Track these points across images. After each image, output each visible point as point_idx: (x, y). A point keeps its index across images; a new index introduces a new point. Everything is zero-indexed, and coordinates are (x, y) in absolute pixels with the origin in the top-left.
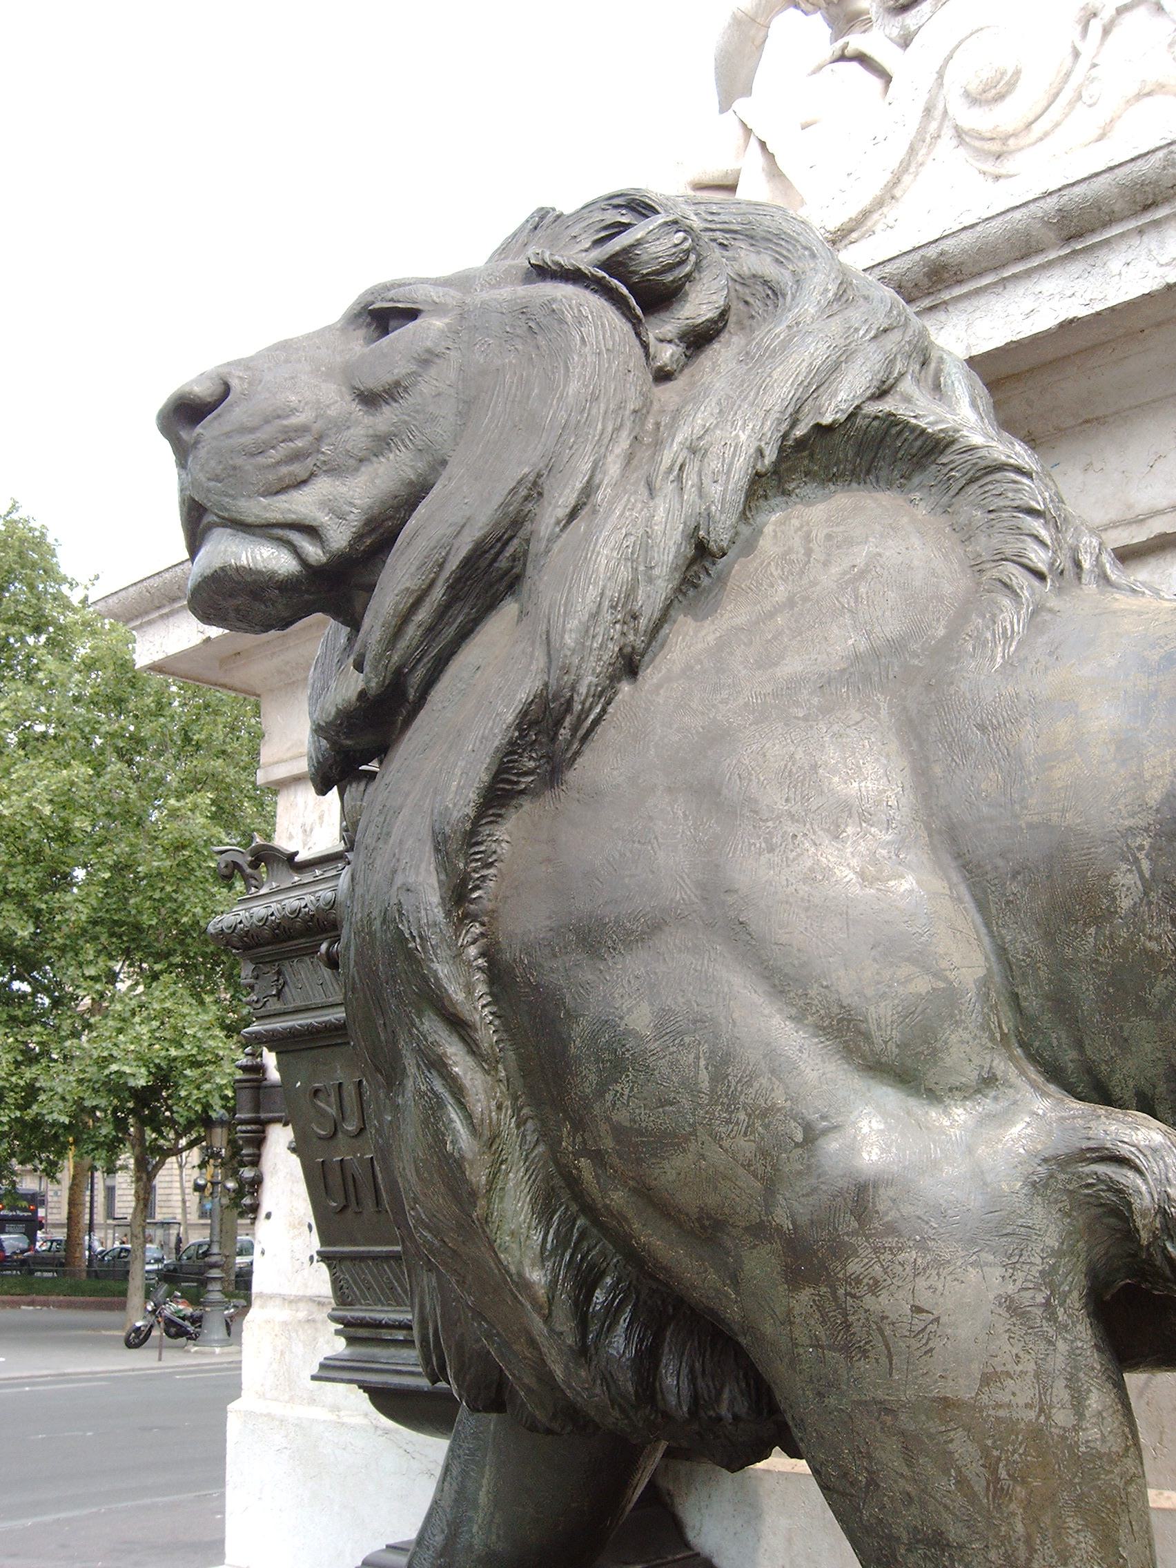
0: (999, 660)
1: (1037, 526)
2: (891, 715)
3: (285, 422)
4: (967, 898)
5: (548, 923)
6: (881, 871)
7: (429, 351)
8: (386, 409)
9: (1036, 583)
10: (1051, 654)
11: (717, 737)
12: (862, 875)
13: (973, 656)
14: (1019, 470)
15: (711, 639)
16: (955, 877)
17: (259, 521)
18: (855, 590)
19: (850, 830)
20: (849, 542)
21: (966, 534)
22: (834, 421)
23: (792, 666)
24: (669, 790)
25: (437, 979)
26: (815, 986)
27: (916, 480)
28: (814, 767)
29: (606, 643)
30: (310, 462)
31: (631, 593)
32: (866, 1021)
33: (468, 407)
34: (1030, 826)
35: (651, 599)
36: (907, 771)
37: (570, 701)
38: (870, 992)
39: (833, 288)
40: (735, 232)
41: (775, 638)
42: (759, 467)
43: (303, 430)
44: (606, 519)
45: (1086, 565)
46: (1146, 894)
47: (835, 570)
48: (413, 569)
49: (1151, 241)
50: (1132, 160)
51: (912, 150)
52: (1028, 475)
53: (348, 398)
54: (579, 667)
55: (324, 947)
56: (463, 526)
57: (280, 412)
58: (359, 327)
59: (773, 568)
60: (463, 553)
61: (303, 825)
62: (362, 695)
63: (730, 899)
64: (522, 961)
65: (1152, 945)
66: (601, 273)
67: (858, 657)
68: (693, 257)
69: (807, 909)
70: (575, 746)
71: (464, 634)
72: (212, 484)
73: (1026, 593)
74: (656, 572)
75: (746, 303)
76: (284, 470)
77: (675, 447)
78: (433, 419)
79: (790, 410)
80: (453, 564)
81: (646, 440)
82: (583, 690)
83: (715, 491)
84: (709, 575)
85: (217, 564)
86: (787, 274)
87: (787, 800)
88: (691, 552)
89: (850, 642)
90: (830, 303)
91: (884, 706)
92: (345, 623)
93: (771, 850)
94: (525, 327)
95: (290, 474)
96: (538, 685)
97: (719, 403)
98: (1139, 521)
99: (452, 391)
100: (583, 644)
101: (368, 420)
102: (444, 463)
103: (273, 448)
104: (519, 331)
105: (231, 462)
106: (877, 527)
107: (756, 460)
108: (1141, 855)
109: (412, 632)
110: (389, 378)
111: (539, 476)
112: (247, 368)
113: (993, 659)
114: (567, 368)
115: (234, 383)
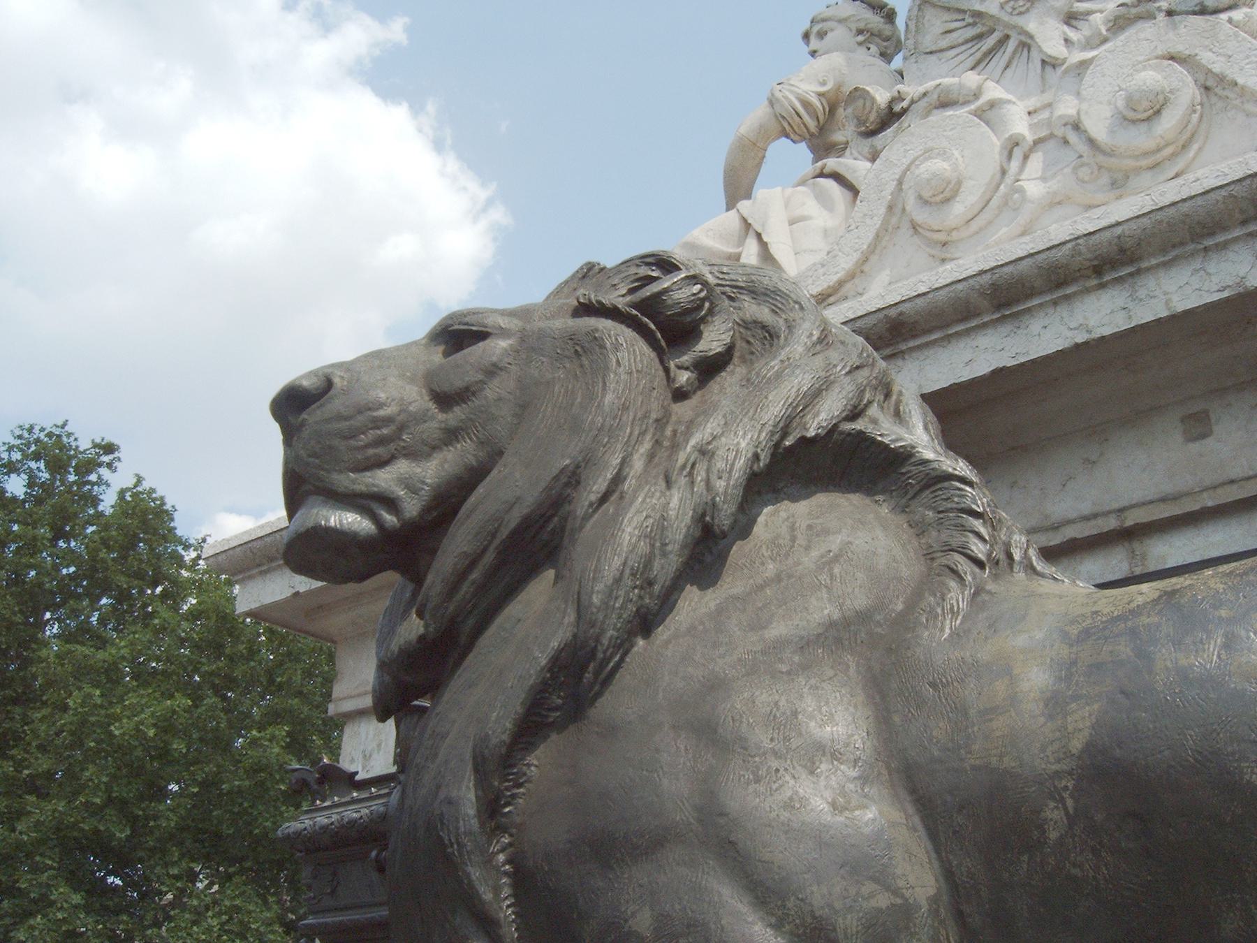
0: (947, 631)
1: (978, 525)
2: (858, 672)
3: (375, 414)
4: (920, 827)
6: (849, 802)
7: (494, 365)
9: (977, 570)
10: (990, 626)
11: (716, 686)
12: (834, 805)
13: (926, 627)
14: (963, 480)
15: (712, 605)
16: (911, 809)
18: (831, 570)
19: (824, 767)
20: (826, 532)
21: (920, 529)
22: (817, 435)
23: (778, 630)
24: (674, 727)
25: (470, 881)
26: (792, 899)
27: (880, 486)
28: (795, 714)
29: (626, 602)
30: (392, 447)
31: (648, 562)
32: (835, 930)
33: (523, 408)
34: (974, 768)
35: (664, 569)
36: (871, 720)
37: (593, 652)
38: (838, 905)
39: (816, 334)
40: (741, 288)
41: (765, 606)
42: (755, 467)
43: (388, 420)
44: (631, 504)
45: (1017, 556)
46: (1071, 828)
47: (815, 553)
49: (1063, 310)
50: (1048, 249)
51: (878, 237)
52: (971, 484)
53: (427, 398)
54: (603, 622)
55: (374, 854)
58: (439, 344)
59: (764, 550)
60: (513, 525)
61: (364, 751)
62: (422, 638)
63: (722, 821)
65: (1074, 871)
66: (635, 312)
67: (831, 625)
68: (707, 305)
69: (786, 832)
70: (597, 688)
71: (511, 592)
72: (311, 460)
73: (969, 578)
74: (669, 548)
75: (748, 342)
76: (371, 451)
77: (689, 449)
79: (781, 425)
80: (504, 533)
81: (665, 441)
82: (605, 642)
83: (720, 485)
84: (711, 553)
85: (310, 523)
86: (781, 322)
87: (772, 740)
88: (698, 533)
89: (826, 612)
90: (814, 345)
91: (853, 666)
92: (411, 580)
93: (757, 781)
95: (375, 455)
96: (569, 635)
97: (724, 416)
98: (1055, 528)
99: (511, 397)
100: (606, 604)
101: (441, 416)
102: (501, 453)
104: (567, 353)
106: (850, 522)
107: (753, 463)
108: (1066, 795)
109: (466, 588)
111: (578, 467)
112: (348, 370)
113: (942, 630)
114: (604, 383)
115: (336, 380)
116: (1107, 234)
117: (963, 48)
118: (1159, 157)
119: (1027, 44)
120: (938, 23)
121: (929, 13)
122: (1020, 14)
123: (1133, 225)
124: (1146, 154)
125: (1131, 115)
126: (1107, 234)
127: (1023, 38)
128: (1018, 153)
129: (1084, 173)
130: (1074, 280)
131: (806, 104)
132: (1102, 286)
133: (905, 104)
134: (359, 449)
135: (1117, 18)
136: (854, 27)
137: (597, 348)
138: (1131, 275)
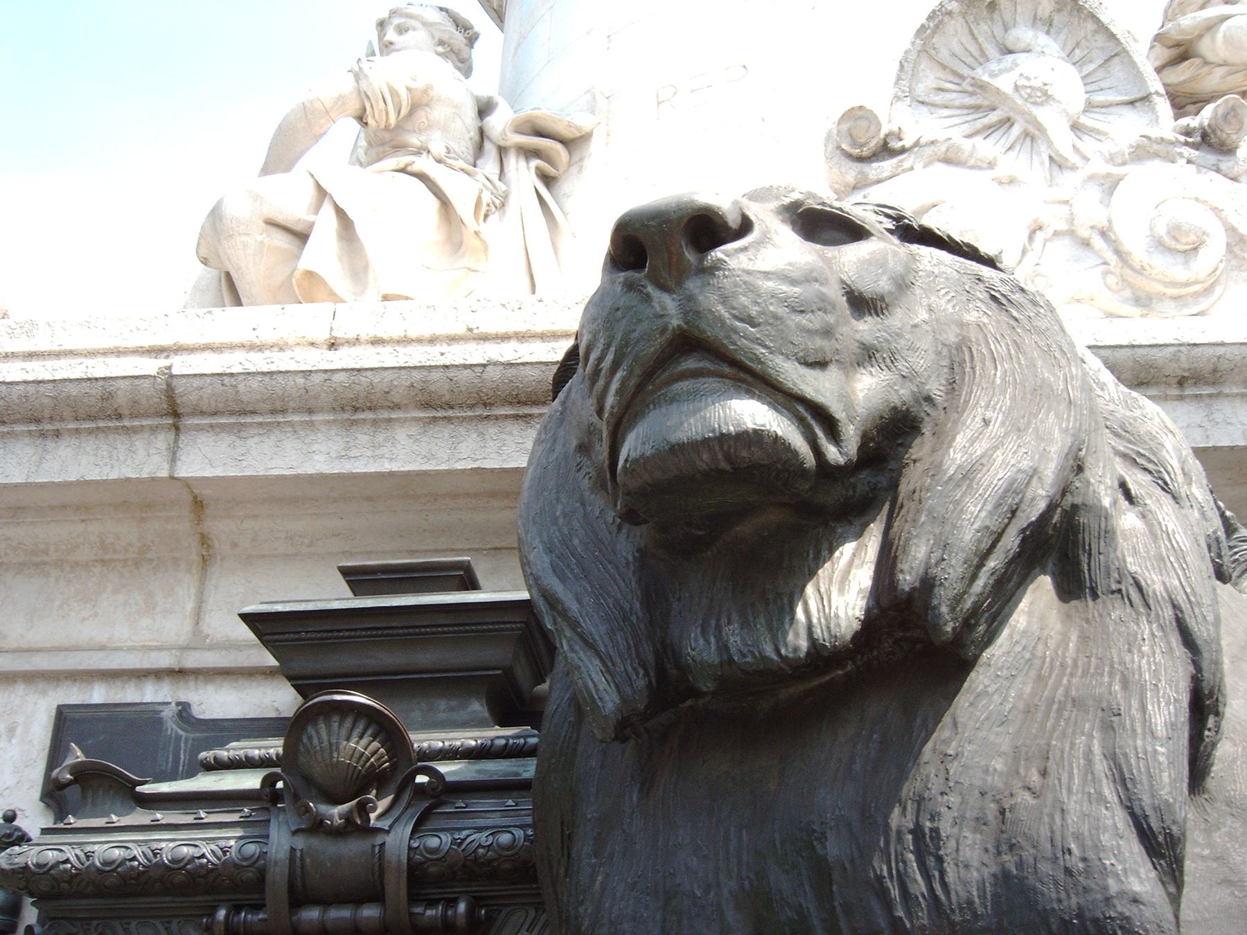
8: (868, 318)
48: (989, 507)
50: (1150, 346)
55: (222, 914)
56: (1032, 477)
57: (815, 274)
60: (1042, 505)
78: (912, 348)
80: (1033, 513)
94: (987, 295)
95: (822, 349)
105: (771, 308)
116: (1210, 351)
117: (958, 112)
118: (1184, 291)
119: (1033, 135)
120: (932, 77)
121: (924, 64)
122: (1035, 103)
123: (1236, 350)
124: (1174, 284)
125: (1168, 241)
126: (1210, 351)
127: (1031, 129)
128: (1039, 236)
129: (1112, 280)
130: (1157, 383)
131: (394, 93)
132: (1181, 398)
133: (907, 143)
134: (809, 331)
135: (1138, 147)
136: (438, 35)
138: (1210, 396)
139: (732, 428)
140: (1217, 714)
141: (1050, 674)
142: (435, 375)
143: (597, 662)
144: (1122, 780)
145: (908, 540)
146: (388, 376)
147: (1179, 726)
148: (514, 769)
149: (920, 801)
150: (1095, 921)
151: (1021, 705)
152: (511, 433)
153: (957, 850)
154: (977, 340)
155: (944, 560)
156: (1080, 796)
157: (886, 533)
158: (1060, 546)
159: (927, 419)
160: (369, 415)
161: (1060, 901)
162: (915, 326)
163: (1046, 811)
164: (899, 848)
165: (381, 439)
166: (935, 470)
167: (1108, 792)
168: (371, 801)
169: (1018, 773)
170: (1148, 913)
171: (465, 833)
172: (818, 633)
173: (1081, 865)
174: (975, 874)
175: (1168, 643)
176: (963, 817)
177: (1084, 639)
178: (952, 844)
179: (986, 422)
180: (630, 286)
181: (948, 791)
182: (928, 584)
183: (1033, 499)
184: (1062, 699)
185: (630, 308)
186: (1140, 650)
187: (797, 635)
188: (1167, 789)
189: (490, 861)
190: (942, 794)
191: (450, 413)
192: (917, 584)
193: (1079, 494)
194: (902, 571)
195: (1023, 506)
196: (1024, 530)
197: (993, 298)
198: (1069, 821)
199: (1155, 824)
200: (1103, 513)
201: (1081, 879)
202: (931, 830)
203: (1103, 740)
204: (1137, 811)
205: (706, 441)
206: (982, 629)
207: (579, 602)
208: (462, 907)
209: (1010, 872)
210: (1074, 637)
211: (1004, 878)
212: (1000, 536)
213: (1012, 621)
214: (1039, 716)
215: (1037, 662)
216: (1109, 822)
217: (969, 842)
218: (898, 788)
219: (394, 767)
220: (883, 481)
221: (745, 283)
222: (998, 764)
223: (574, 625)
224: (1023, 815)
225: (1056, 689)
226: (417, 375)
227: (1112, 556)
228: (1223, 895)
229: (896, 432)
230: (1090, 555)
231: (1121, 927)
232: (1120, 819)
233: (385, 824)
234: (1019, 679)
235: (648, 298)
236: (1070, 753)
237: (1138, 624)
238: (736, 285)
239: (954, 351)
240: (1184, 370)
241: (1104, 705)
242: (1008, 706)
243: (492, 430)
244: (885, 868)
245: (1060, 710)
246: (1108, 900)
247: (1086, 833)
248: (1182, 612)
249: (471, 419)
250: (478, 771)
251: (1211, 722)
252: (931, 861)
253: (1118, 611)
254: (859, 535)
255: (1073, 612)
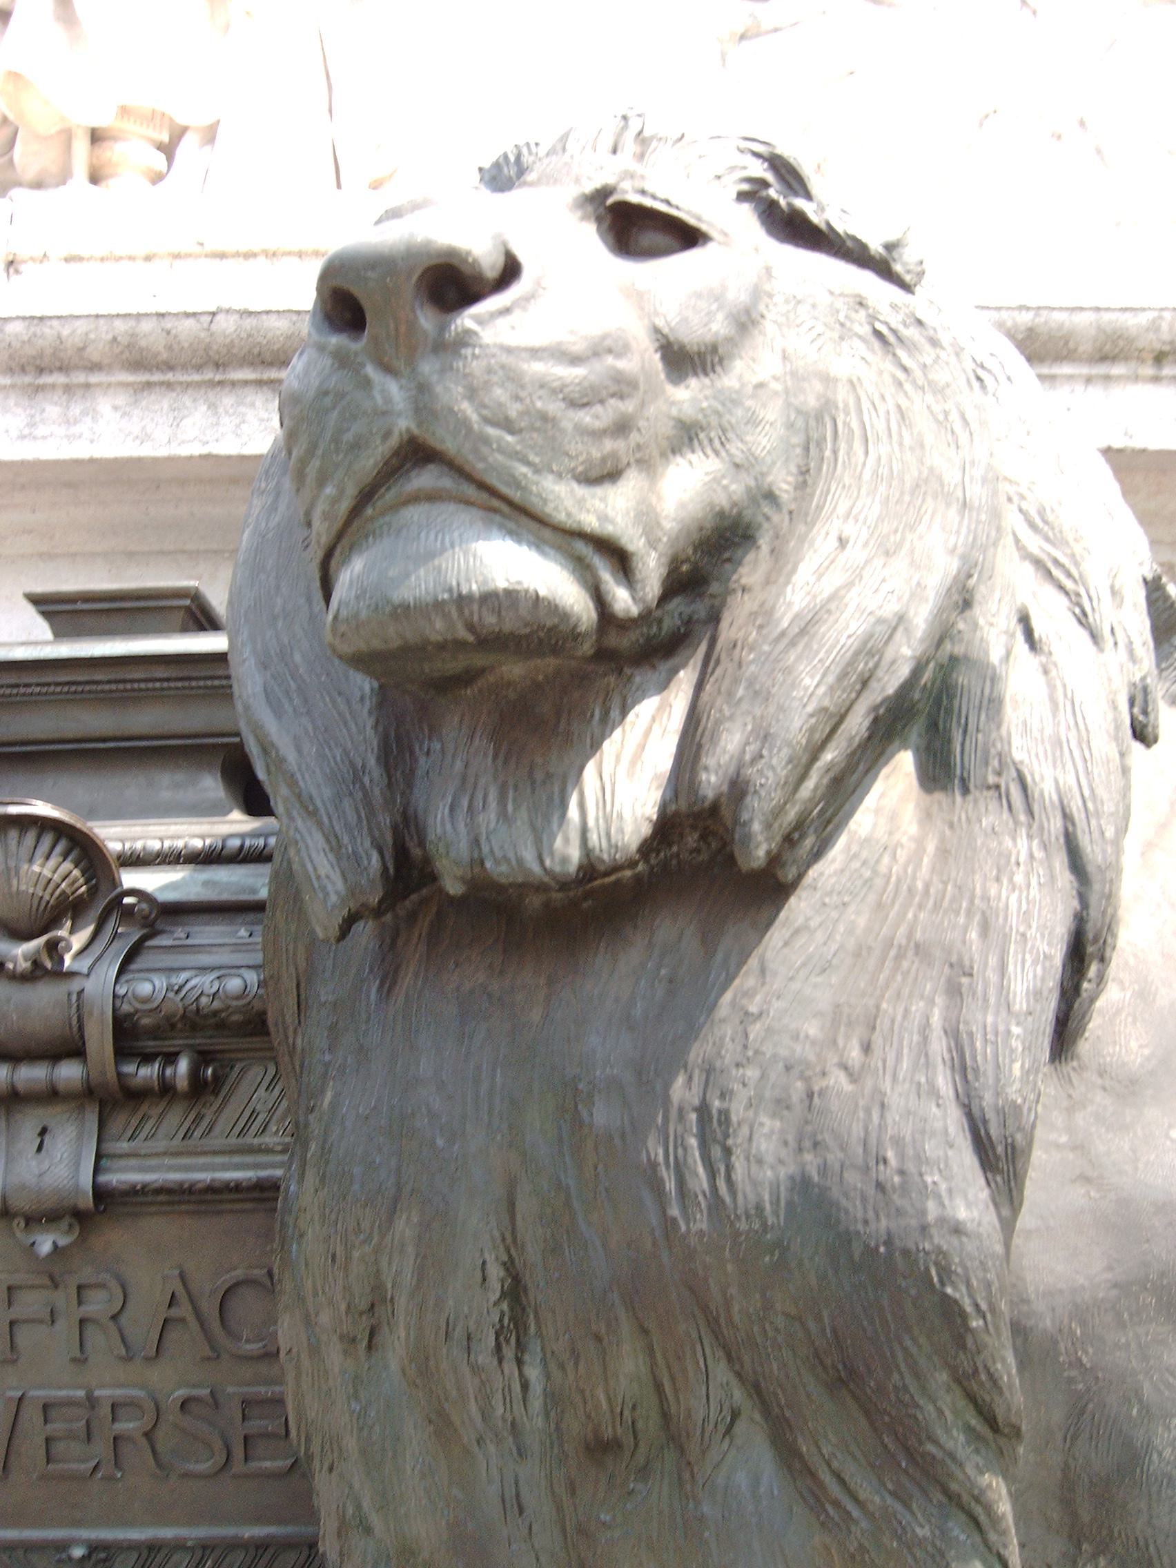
5: (1109, 1276)
7: (748, 312)
8: (693, 382)
17: (570, 524)
48: (831, 679)
56: (895, 629)
57: (608, 342)
60: (904, 671)
64: (1071, 1332)
72: (491, 431)
76: (609, 445)
78: (753, 421)
80: (890, 683)
95: (614, 455)
103: (602, 402)
105: (539, 404)
110: (708, 338)
130: (1126, 359)
132: (1156, 379)
137: (927, 347)
139: (474, 587)
140: (1102, 959)
141: (893, 902)
142: (146, 326)
143: (319, 837)
144: (963, 1068)
145: (718, 723)
146: (81, 327)
147: (1045, 993)
148: (250, 881)
149: (709, 1071)
150: (906, 1253)
151: (851, 944)
152: (252, 405)
153: (750, 1139)
154: (846, 405)
155: (761, 756)
156: (907, 1085)
157: (699, 687)
158: (929, 716)
159: (766, 525)
160: (59, 379)
161: (866, 1222)
162: (760, 386)
163: (861, 1103)
164: (680, 1129)
165: (77, 411)
166: (765, 615)
167: (944, 1082)
168: (60, 939)
169: (835, 1042)
170: (970, 1246)
171: (183, 976)
172: (594, 839)
173: (897, 1179)
174: (769, 1173)
175: (1051, 869)
176: (760, 1097)
177: (943, 853)
178: (745, 1130)
179: (842, 542)
180: (342, 360)
181: (745, 1061)
182: (738, 789)
183: (893, 662)
184: (904, 942)
185: (341, 395)
186: (1011, 880)
187: (567, 840)
188: (1017, 1086)
189: (215, 1013)
190: (738, 1065)
191: (170, 376)
192: (725, 788)
193: (961, 640)
194: (706, 769)
195: (880, 673)
196: (875, 708)
197: (878, 334)
198: (889, 1121)
199: (994, 1131)
200: (990, 672)
201: (895, 1197)
202: (720, 1112)
203: (947, 1008)
204: (976, 1112)
205: (438, 605)
206: (809, 842)
207: (299, 750)
208: (183, 1066)
209: (810, 1178)
210: (931, 847)
211: (802, 1184)
212: (842, 718)
213: (852, 824)
214: (872, 963)
215: (879, 882)
216: (938, 1125)
217: (766, 1130)
218: (685, 1051)
219: (93, 891)
220: (700, 609)
221: (503, 367)
222: (813, 1029)
223: (292, 783)
224: (834, 1105)
225: (897, 926)
226: (121, 326)
227: (994, 735)
228: (1077, 1196)
229: (714, 554)
230: (965, 732)
231: (936, 1264)
232: (952, 1121)
233: (84, 965)
234: (852, 908)
235: (366, 384)
236: (901, 1026)
237: (1014, 839)
238: (489, 371)
239: (812, 423)
240: (1164, 343)
241: (954, 959)
242: (834, 947)
243: (227, 400)
244: (661, 1152)
245: (899, 957)
246: (924, 1229)
247: (908, 1139)
248: (1074, 824)
249: (199, 385)
250: (206, 884)
251: (1093, 970)
252: (716, 1152)
253: (991, 816)
254: (664, 686)
255: (935, 808)
